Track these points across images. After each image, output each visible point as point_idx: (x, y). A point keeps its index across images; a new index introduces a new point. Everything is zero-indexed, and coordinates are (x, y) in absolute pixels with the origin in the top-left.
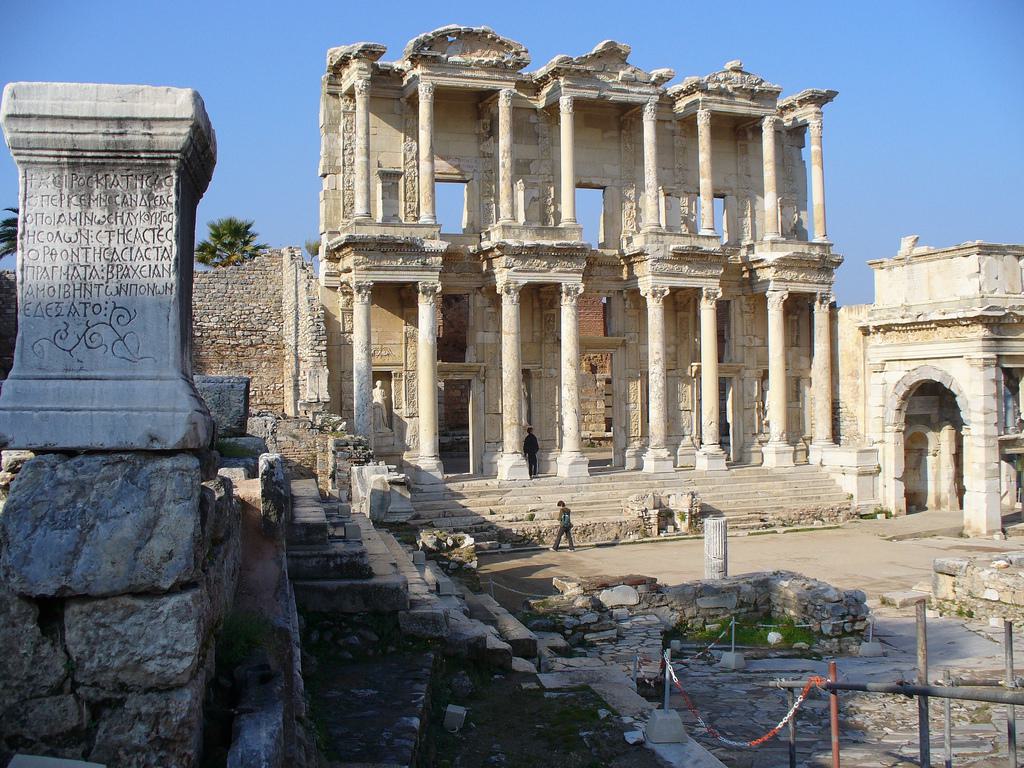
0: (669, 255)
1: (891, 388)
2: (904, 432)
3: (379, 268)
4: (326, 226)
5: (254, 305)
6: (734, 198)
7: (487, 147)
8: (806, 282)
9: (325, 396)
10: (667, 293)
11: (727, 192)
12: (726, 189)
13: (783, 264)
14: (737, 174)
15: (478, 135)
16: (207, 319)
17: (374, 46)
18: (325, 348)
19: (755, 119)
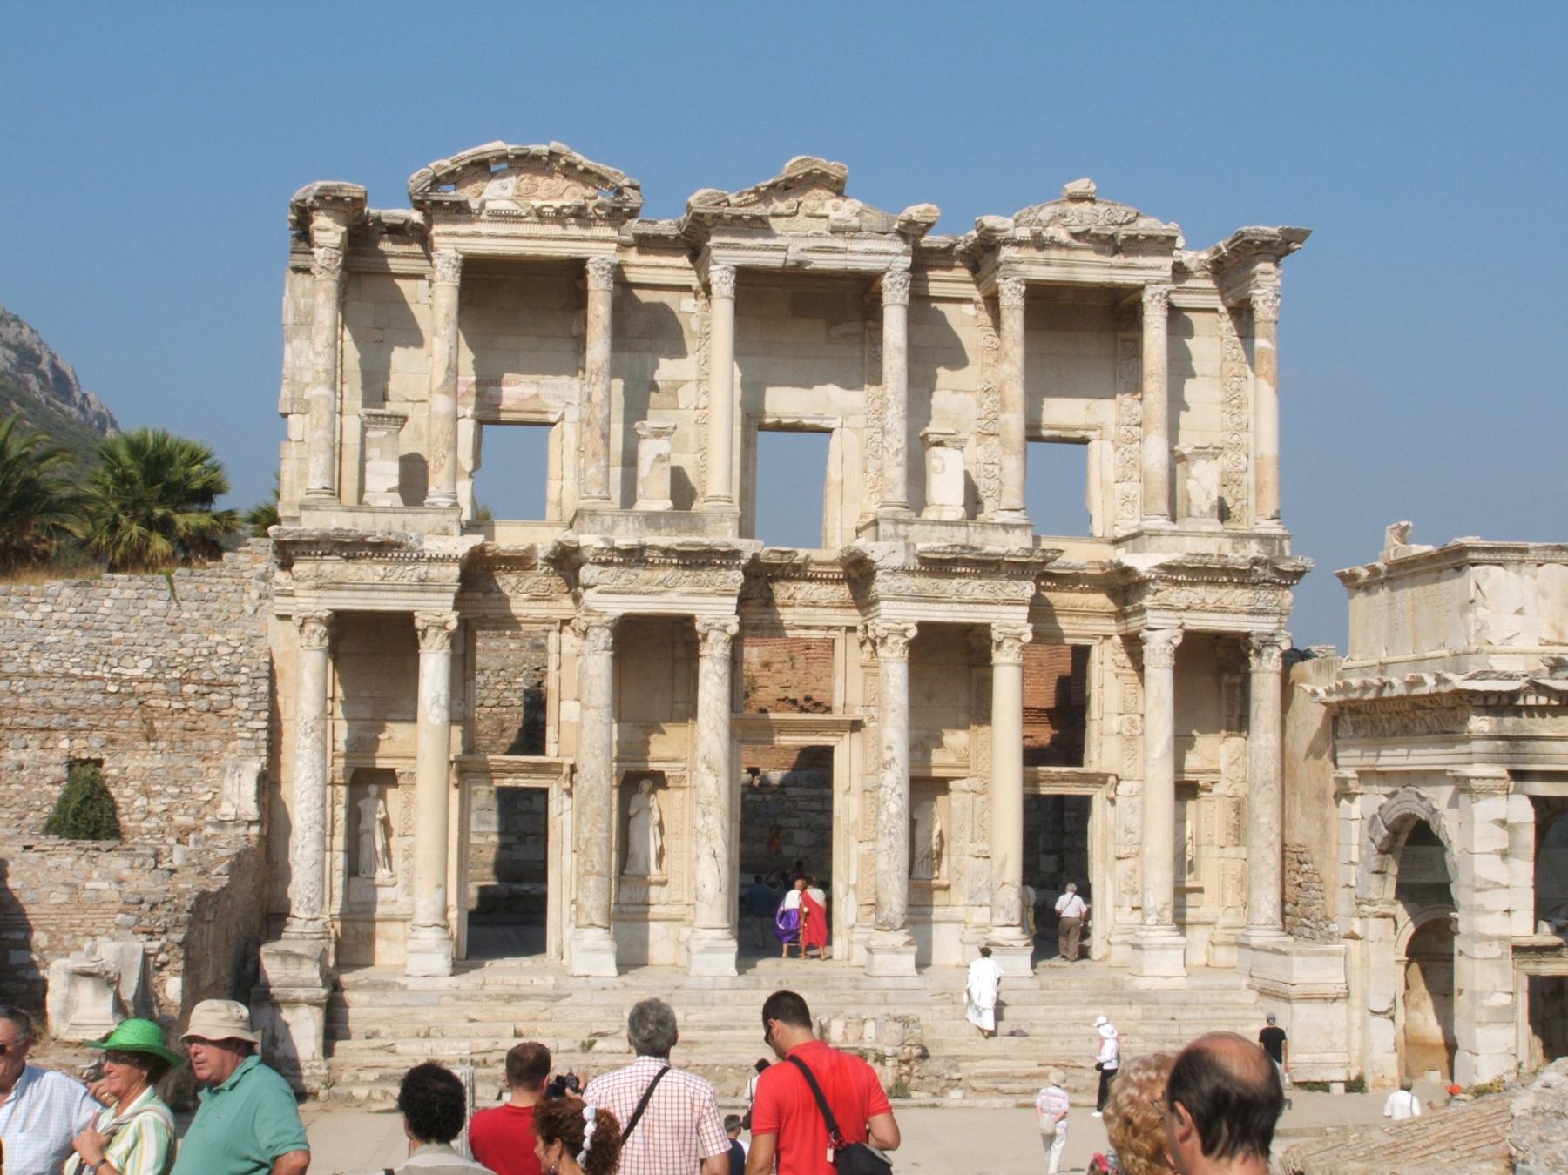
3: (338, 585)
5: (218, 638)
6: (1107, 444)
8: (1223, 610)
9: (251, 810)
11: (1090, 434)
16: (128, 661)
17: (340, 189)
18: (264, 724)
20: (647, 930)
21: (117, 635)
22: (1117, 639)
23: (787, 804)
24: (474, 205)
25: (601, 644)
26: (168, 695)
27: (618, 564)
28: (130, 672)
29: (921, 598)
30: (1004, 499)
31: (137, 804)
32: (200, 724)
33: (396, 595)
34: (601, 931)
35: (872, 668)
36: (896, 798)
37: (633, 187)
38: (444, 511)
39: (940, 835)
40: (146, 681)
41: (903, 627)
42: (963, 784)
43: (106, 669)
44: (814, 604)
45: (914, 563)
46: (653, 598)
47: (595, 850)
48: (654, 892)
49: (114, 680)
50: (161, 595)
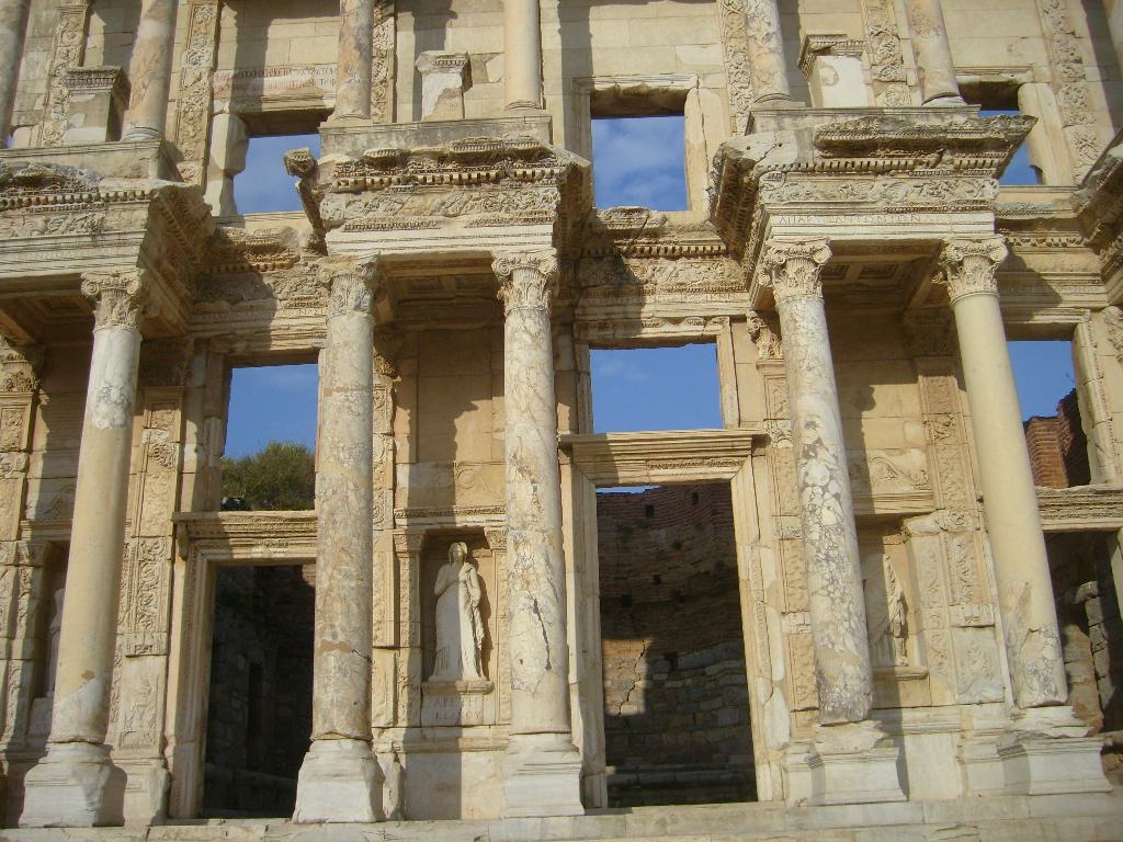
6: (1042, 87)
10: (824, 256)
11: (1019, 77)
12: (1014, 70)
20: (458, 765)
22: (1115, 310)
23: (708, 685)
25: (352, 302)
27: (372, 188)
29: (833, 207)
30: (929, 86)
33: (58, 255)
34: (348, 744)
35: (778, 371)
36: (832, 502)
39: (902, 600)
41: (807, 248)
42: (928, 523)
44: (681, 288)
46: (428, 233)
47: (338, 607)
48: (470, 707)
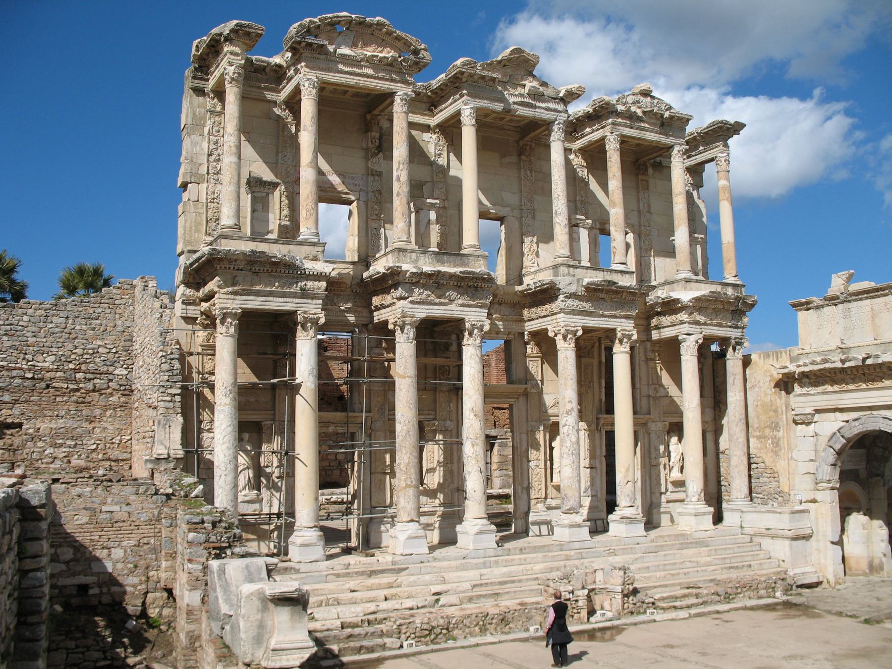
0: (581, 291)
1: (823, 441)
2: (838, 489)
3: (249, 293)
4: (186, 243)
5: (99, 343)
7: (377, 164)
8: (720, 325)
10: (580, 333)
13: (700, 305)
14: (639, 211)
15: (367, 150)
16: (40, 358)
17: (249, 27)
18: (179, 391)
19: (663, 148)
21: (32, 340)
24: (331, 48)
26: (66, 380)
28: (40, 364)
31: (47, 452)
32: (88, 399)
37: (425, 50)
38: (314, 244)
40: (52, 370)
43: (24, 362)
45: (581, 291)
49: (30, 370)
50: (61, 314)
